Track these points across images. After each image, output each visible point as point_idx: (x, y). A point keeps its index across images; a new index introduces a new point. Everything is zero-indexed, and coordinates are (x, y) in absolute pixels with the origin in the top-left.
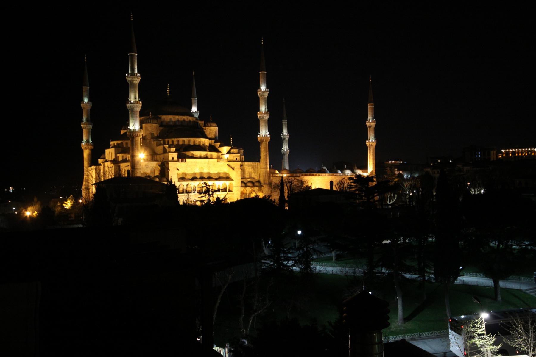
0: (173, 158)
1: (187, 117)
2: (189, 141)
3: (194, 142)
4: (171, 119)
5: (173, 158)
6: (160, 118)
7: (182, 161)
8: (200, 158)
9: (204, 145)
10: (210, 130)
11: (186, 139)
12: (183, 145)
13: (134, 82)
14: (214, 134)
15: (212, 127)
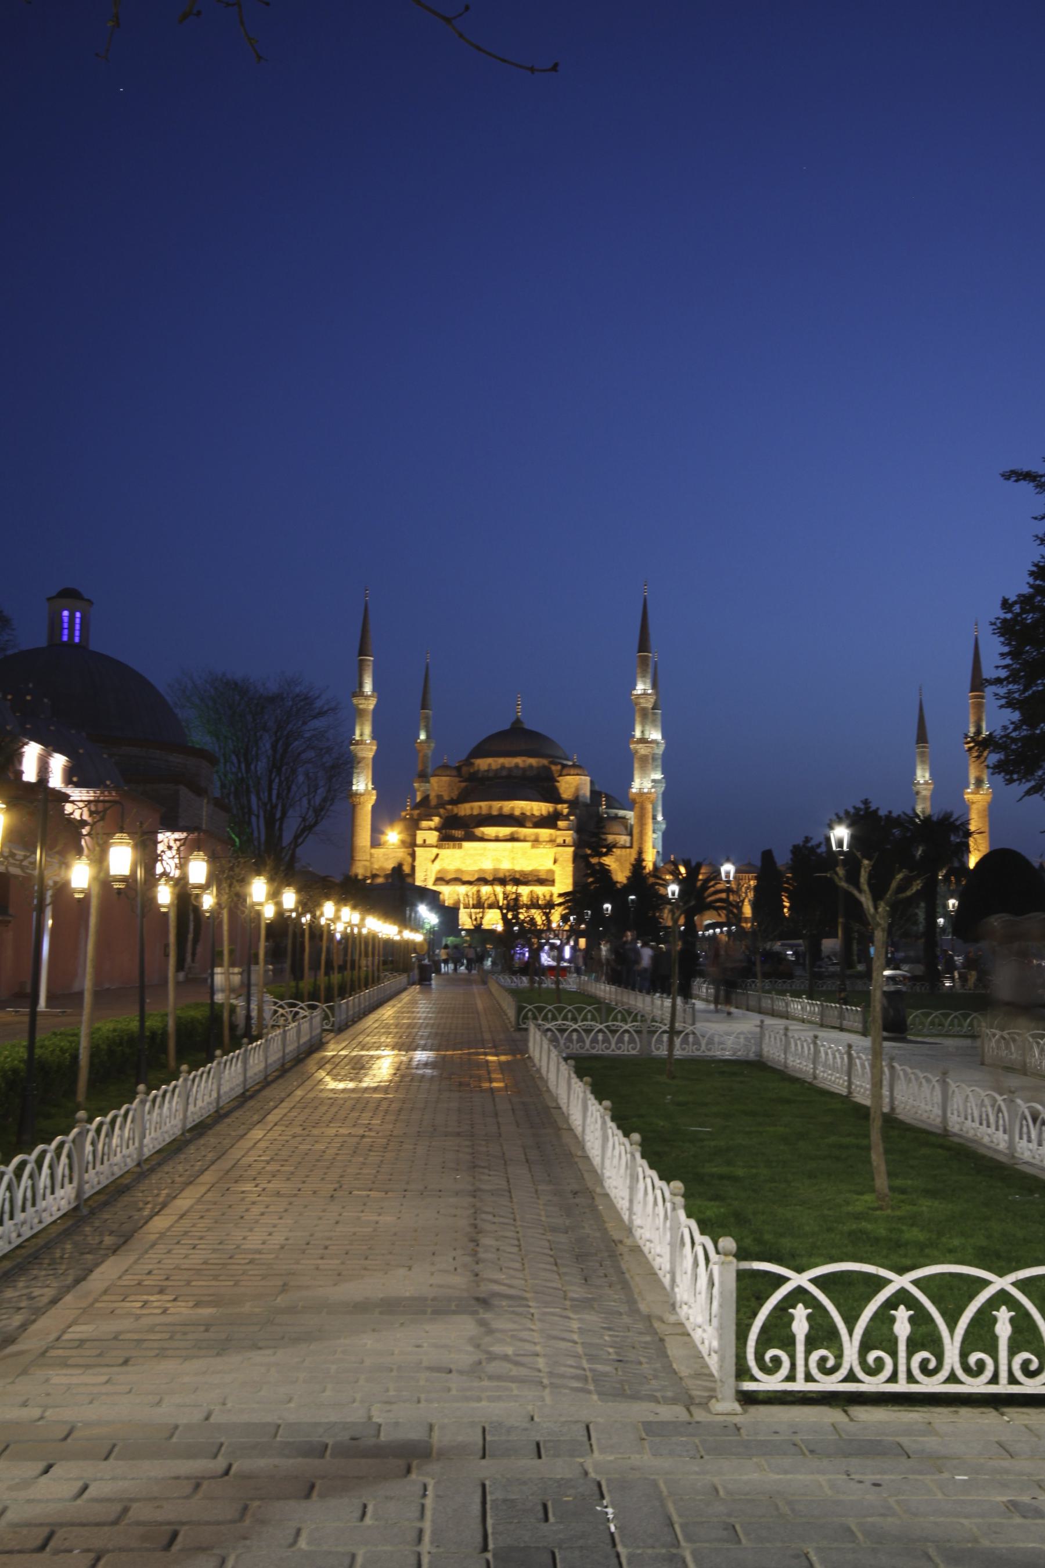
0: (425, 841)
1: (524, 758)
2: (490, 807)
3: (501, 808)
4: (490, 765)
5: (425, 841)
6: (472, 764)
7: (454, 847)
8: (497, 840)
9: (523, 814)
10: (566, 783)
11: (483, 804)
12: (479, 815)
13: (361, 706)
14: (573, 790)
15: (568, 777)
